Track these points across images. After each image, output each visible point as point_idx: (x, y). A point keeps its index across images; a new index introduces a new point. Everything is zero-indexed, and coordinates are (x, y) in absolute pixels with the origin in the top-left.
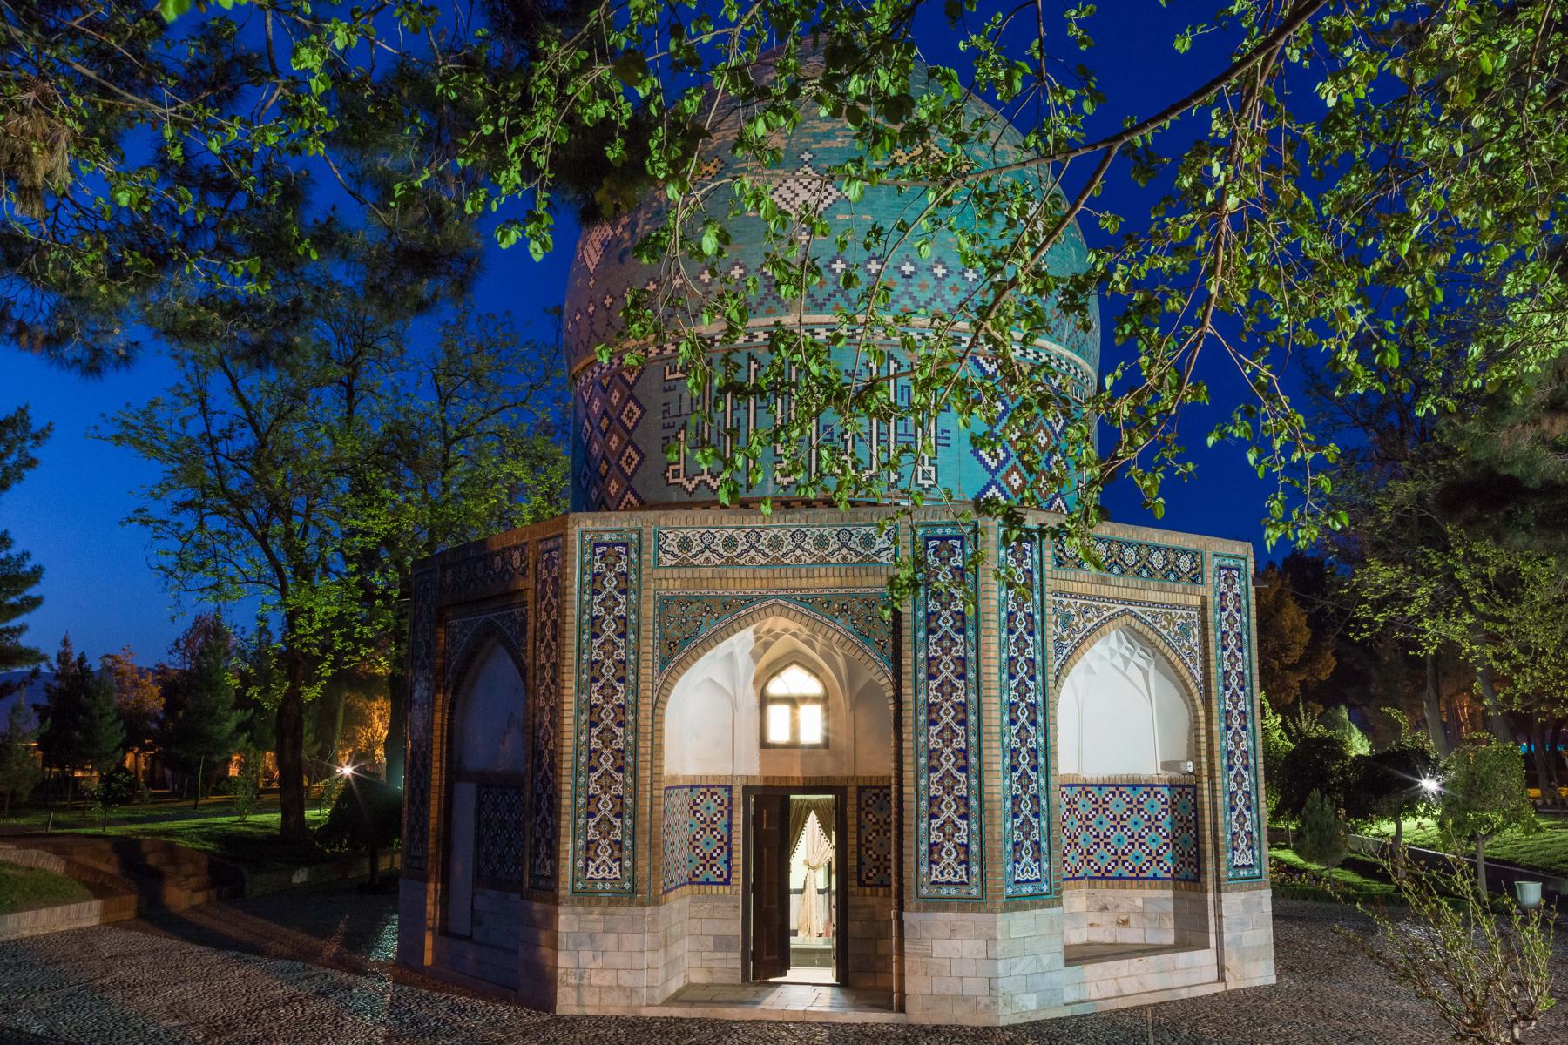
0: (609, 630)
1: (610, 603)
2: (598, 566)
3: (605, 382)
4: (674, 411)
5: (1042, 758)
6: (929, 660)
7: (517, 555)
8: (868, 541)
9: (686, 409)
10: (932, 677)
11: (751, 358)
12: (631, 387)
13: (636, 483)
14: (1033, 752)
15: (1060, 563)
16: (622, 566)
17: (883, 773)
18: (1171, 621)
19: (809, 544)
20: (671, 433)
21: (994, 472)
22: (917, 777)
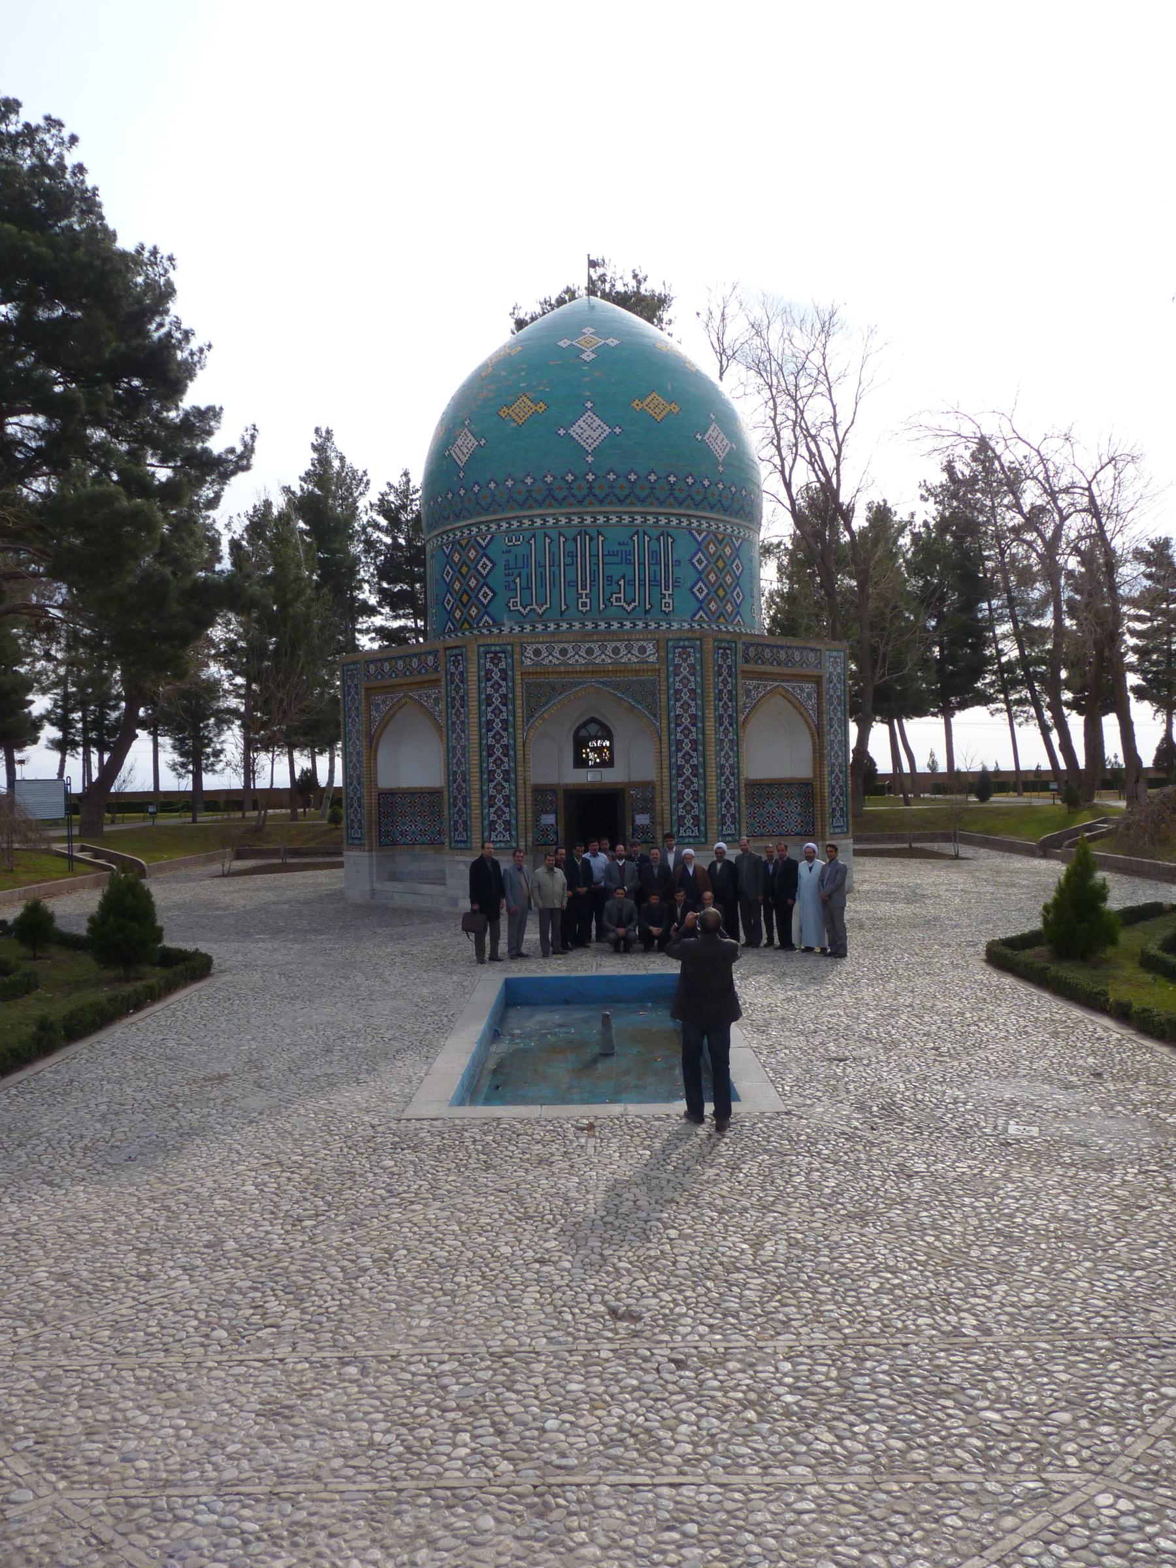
0: (497, 702)
1: (497, 686)
2: (489, 666)
3: (464, 543)
4: (512, 565)
5: (736, 769)
6: (678, 716)
7: (431, 658)
8: (642, 650)
9: (520, 564)
10: (678, 725)
11: (560, 534)
12: (484, 548)
13: (490, 609)
14: (732, 766)
15: (747, 662)
16: (503, 665)
17: (648, 778)
18: (802, 690)
19: (609, 651)
20: (511, 578)
21: (701, 602)
22: (671, 780)
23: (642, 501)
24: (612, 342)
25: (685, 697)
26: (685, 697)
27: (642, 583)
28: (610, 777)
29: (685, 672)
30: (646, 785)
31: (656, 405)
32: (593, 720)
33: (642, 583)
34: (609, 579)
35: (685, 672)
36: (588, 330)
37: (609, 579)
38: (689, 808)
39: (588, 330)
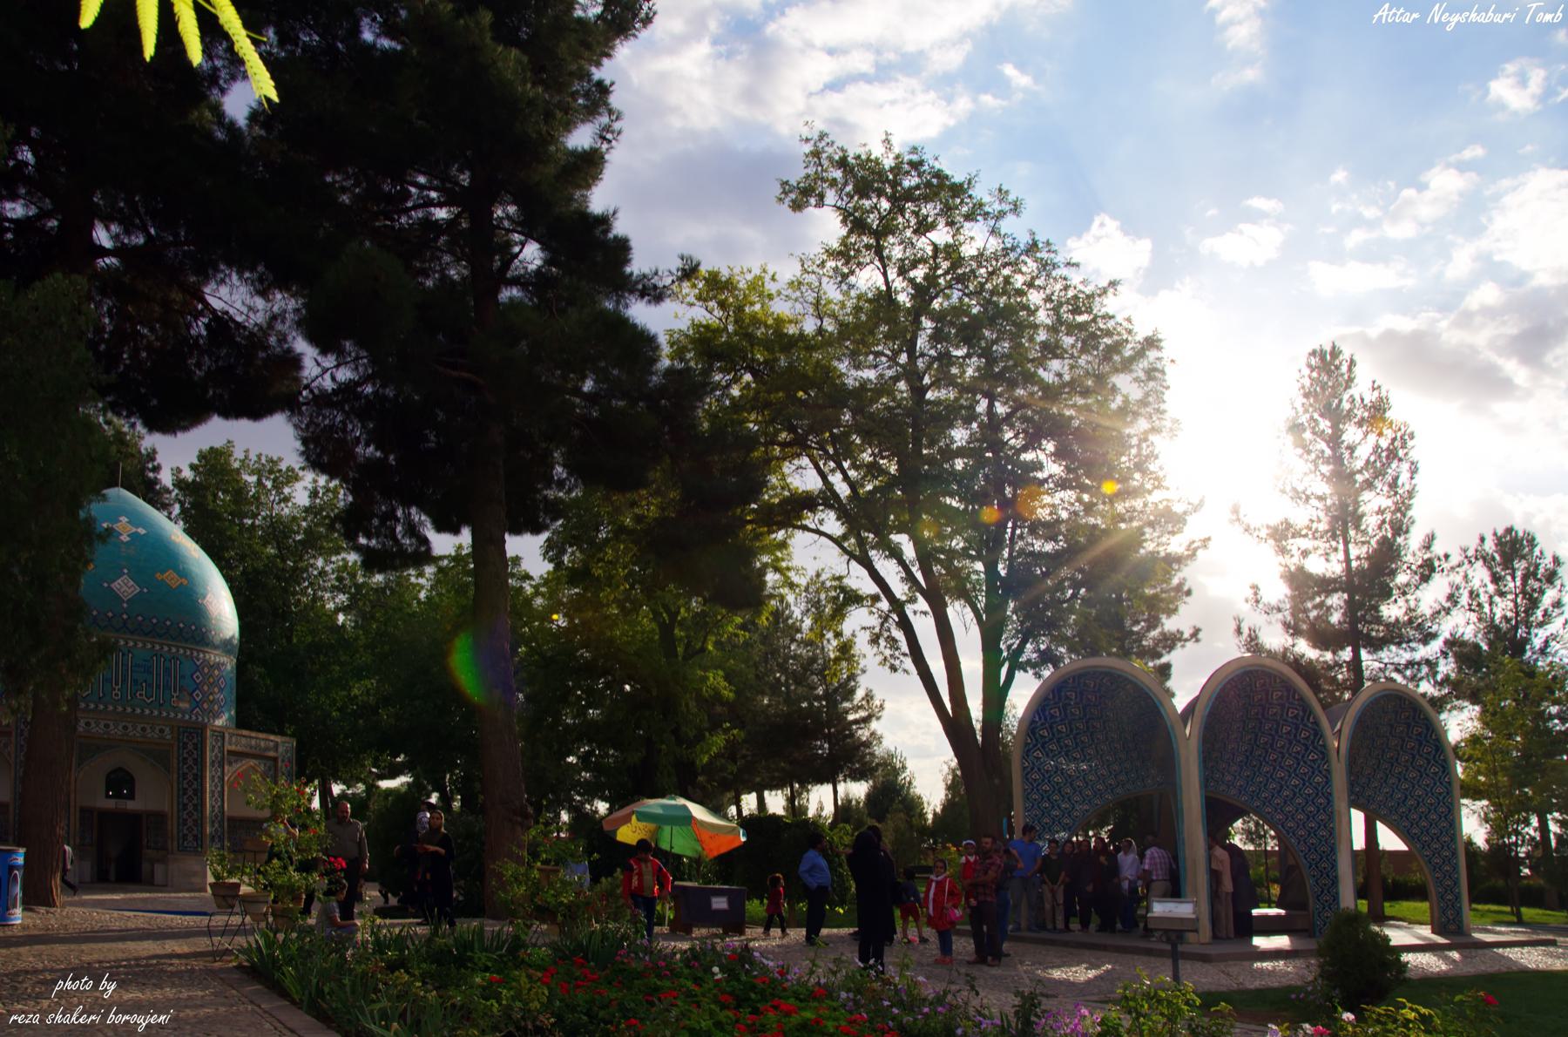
23: (160, 636)
24: (142, 531)
25: (190, 762)
26: (190, 762)
27: (158, 686)
28: (131, 805)
29: (190, 747)
30: (159, 818)
31: (170, 577)
32: (120, 769)
33: (158, 686)
34: (135, 681)
35: (190, 747)
36: (124, 519)
37: (135, 681)
38: (190, 829)
39: (124, 519)
